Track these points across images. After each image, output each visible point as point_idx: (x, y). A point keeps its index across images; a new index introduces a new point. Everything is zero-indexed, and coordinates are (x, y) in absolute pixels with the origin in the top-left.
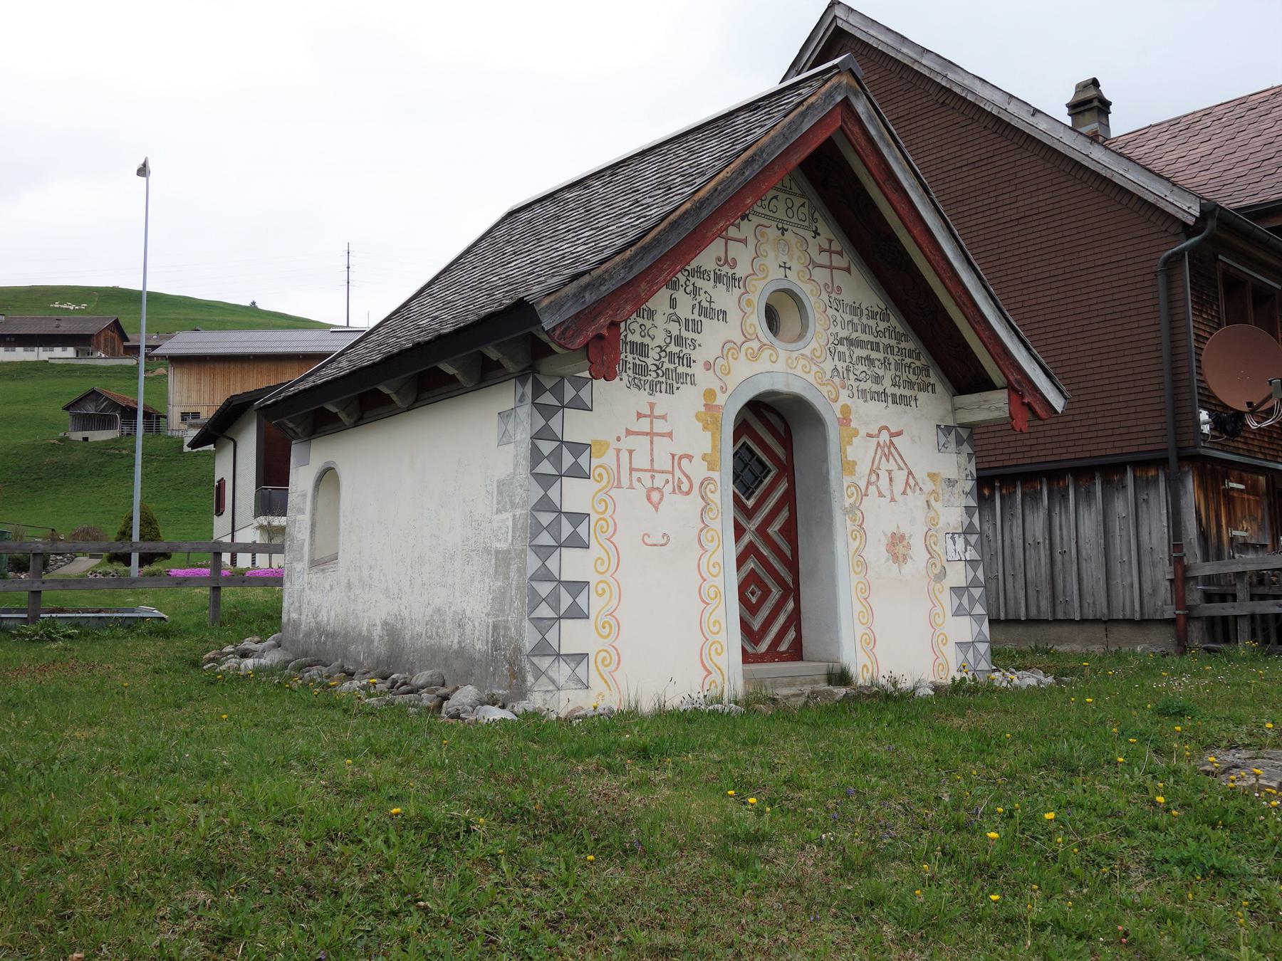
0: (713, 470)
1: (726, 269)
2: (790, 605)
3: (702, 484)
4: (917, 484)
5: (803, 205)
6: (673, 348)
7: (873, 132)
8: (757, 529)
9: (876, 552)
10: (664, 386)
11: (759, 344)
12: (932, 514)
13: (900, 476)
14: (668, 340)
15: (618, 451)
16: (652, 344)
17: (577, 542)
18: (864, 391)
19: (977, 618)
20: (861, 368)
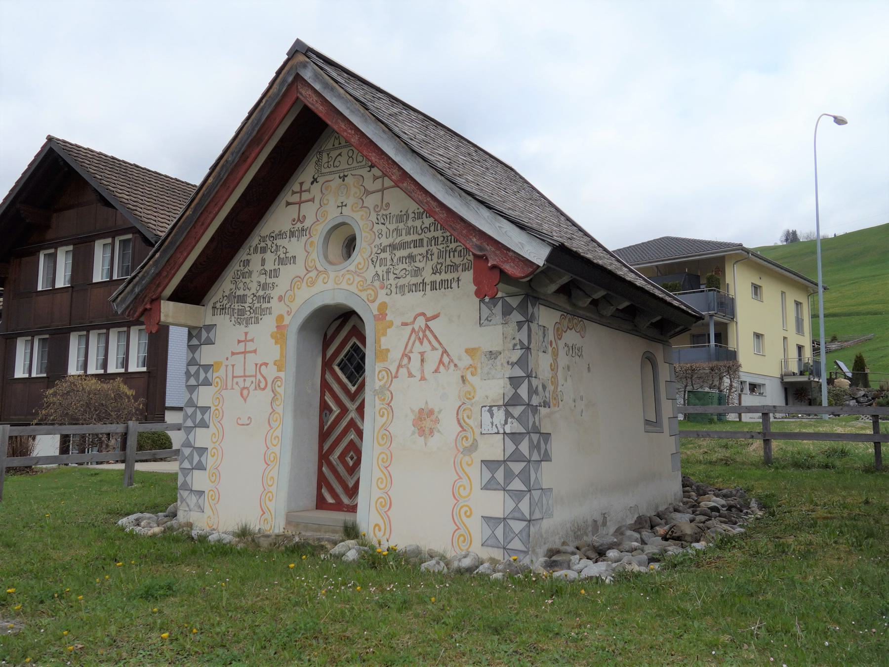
4: (451, 361)
7: (317, 87)
9: (402, 427)
13: (433, 358)
15: (227, 366)
18: (402, 287)
20: (401, 266)
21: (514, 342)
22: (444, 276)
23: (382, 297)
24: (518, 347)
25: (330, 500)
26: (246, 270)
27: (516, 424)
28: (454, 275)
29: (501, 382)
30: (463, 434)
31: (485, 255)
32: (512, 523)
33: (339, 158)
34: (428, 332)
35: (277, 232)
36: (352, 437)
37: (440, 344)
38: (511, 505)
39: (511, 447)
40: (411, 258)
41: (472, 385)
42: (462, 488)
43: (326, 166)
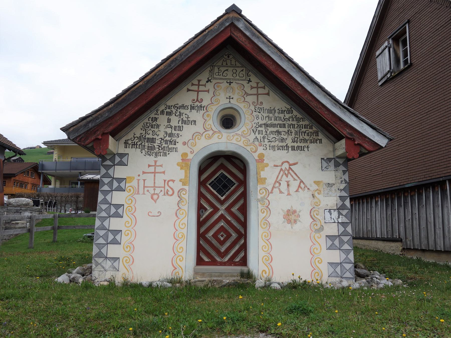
0: (185, 185)
1: (197, 103)
2: (242, 241)
3: (179, 191)
5: (242, 71)
6: (168, 138)
7: (248, 34)
8: (225, 209)
9: (276, 219)
10: (162, 154)
11: (212, 132)
12: (316, 200)
13: (295, 185)
14: (165, 135)
15: (138, 180)
16: (157, 138)
17: (118, 215)
18: (273, 147)
19: (347, 252)
20: (272, 136)
21: (341, 179)
23: (260, 150)
25: (206, 259)
26: (154, 123)
27: (344, 218)
28: (306, 144)
29: (335, 198)
30: (314, 223)
34: (290, 171)
35: (180, 104)
36: (222, 224)
37: (299, 178)
38: (344, 256)
39: (342, 229)
40: (279, 132)
42: (315, 250)
43: (217, 74)
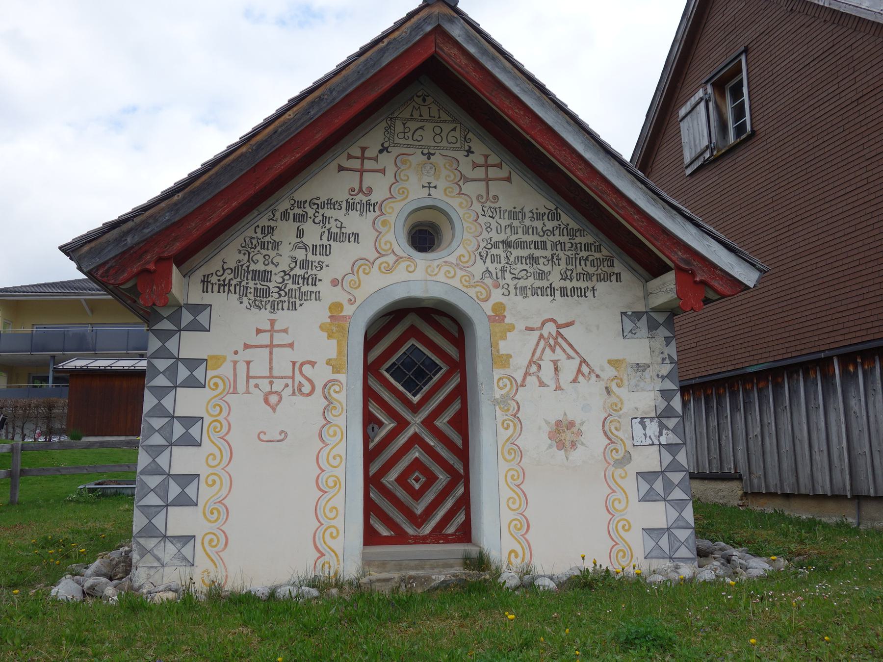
0: (338, 372)
1: (360, 197)
2: (460, 490)
3: (325, 386)
4: (592, 371)
5: (454, 129)
6: (298, 271)
7: (472, 50)
8: (422, 422)
9: (535, 440)
10: (286, 305)
11: (394, 258)
12: (613, 399)
13: (569, 368)
14: (293, 265)
16: (275, 270)
17: (189, 441)
19: (679, 505)
20: (520, 267)
21: (662, 356)
22: (575, 283)
23: (497, 296)
24: (667, 361)
25: (384, 532)
26: (268, 239)
27: (671, 435)
28: (589, 284)
29: (652, 394)
30: (612, 446)
31: (691, 270)
32: (677, 532)
33: (420, 132)
34: (560, 340)
35: (324, 199)
36: (417, 455)
37: (577, 353)
38: (673, 514)
39: (668, 458)
40: (533, 259)
41: (618, 397)
42: (616, 502)
43: (401, 135)
